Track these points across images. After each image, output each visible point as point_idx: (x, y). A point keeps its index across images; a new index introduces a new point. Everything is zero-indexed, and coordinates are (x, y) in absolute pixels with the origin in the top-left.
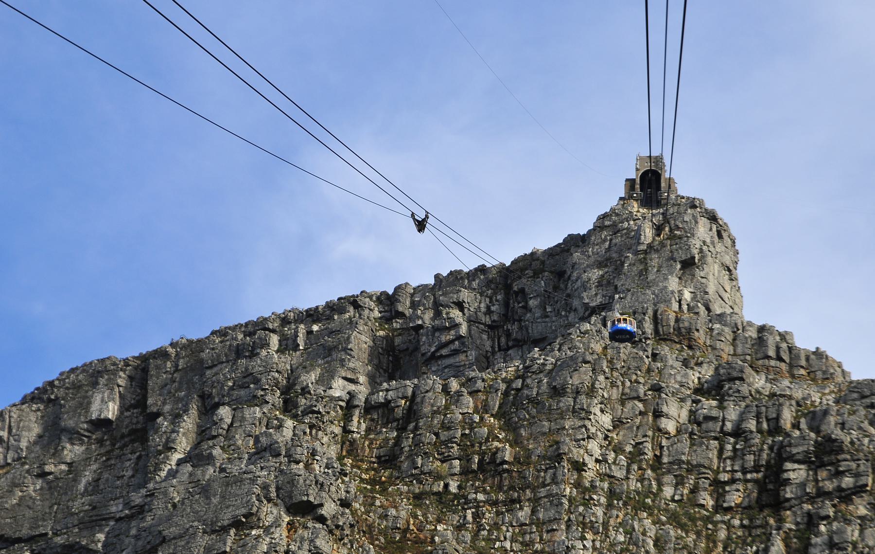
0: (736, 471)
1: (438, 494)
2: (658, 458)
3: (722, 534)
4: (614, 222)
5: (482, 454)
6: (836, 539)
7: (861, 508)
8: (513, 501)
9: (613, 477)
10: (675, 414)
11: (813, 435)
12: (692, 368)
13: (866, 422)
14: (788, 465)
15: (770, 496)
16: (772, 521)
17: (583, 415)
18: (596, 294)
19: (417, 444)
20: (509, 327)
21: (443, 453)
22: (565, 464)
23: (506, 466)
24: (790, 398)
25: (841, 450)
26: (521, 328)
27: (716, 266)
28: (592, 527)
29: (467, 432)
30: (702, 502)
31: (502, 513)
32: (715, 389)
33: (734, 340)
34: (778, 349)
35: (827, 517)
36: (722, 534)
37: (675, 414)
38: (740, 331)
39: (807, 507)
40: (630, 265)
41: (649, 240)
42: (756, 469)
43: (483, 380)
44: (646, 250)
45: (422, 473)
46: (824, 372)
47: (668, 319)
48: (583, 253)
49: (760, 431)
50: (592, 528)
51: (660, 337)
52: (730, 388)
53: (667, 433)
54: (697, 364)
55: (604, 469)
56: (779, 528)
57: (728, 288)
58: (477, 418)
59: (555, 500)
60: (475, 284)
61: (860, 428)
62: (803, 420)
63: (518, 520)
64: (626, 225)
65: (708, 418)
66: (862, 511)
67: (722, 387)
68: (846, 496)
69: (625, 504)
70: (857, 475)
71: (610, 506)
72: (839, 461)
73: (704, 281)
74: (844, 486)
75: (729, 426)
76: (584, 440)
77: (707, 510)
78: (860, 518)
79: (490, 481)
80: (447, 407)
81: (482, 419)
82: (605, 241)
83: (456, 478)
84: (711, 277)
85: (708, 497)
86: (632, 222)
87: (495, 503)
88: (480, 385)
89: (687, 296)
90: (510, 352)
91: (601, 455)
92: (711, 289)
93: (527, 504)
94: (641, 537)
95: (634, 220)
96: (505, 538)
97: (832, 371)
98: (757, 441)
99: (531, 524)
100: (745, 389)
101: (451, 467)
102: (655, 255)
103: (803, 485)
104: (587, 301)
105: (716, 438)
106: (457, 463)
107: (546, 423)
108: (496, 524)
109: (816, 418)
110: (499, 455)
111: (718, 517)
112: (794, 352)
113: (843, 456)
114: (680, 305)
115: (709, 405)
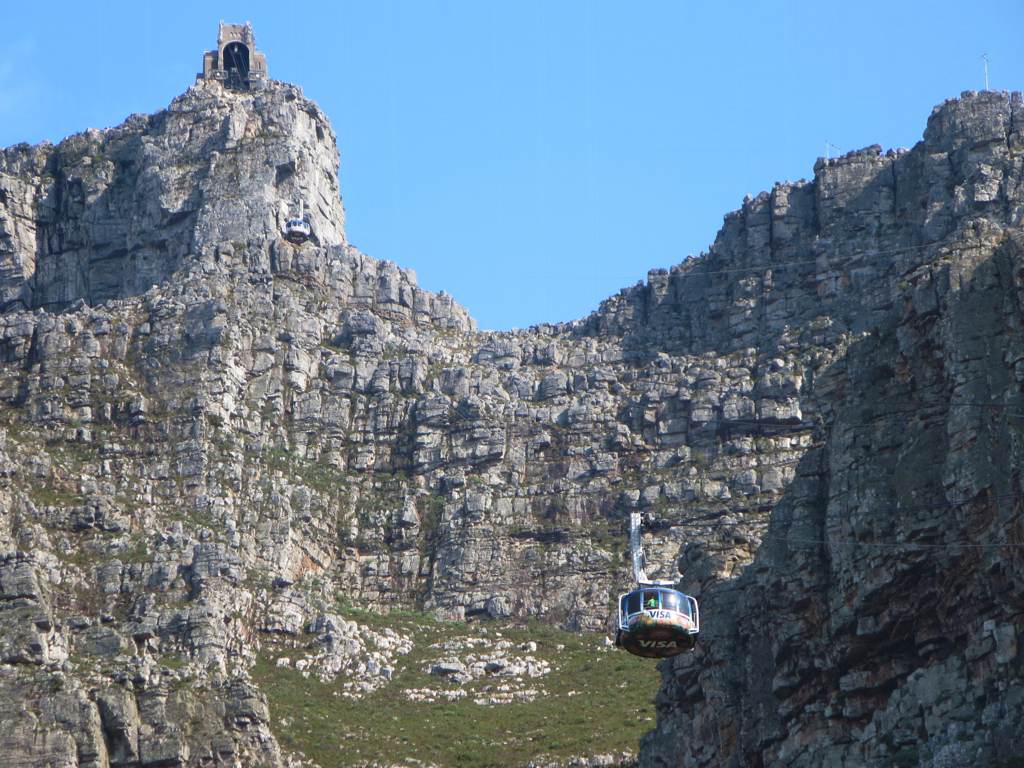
0: (369, 432)
1: (72, 441)
2: (289, 414)
3: (355, 497)
4: (195, 107)
5: (115, 403)
6: (469, 507)
7: (494, 476)
8: (150, 454)
9: (249, 433)
10: (306, 366)
11: (448, 398)
12: (317, 315)
13: (501, 386)
14: (422, 429)
15: (404, 459)
16: (404, 485)
17: (219, 367)
18: (177, 199)
19: (45, 387)
20: (63, 226)
21: (73, 399)
22: (202, 418)
23: (141, 417)
24: (421, 354)
25: (476, 416)
26: (77, 228)
27: (318, 174)
28: (231, 483)
29: (97, 377)
30: (334, 462)
31: (139, 465)
32: (347, 340)
33: (354, 279)
34: (401, 291)
35: (460, 484)
36: (355, 497)
37: (306, 366)
38: (359, 269)
39: (441, 473)
40: (217, 166)
41: (239, 136)
42: (389, 430)
43: (109, 322)
44: (235, 148)
45: (53, 419)
46: (450, 320)
47: (286, 254)
48: (156, 143)
49: (392, 390)
50: (232, 485)
51: (281, 276)
52: (362, 342)
53: (298, 387)
54: (319, 309)
55: (237, 423)
56: (412, 493)
57: (329, 201)
58: (106, 363)
59: (194, 456)
60: (17, 167)
61: (495, 393)
62: (436, 381)
63: (156, 473)
64: (208, 112)
65: (340, 375)
66: (496, 480)
67: (351, 340)
68: (480, 465)
69: (262, 461)
70: (491, 444)
71: (247, 463)
72: (474, 428)
73: (303, 191)
74: (478, 453)
75: (361, 383)
76: (220, 393)
77: (339, 471)
78: (493, 486)
79: (124, 429)
80: (73, 350)
81: (111, 364)
82: (183, 131)
83: (87, 426)
84: (311, 188)
85: (340, 458)
86: (216, 110)
87: (132, 455)
88: (105, 326)
89: (285, 209)
90: (64, 256)
91: (236, 409)
92: (312, 201)
93: (165, 457)
94: (280, 496)
95: (219, 108)
96: (145, 490)
97: (457, 319)
98: (390, 401)
99: (171, 477)
100: (377, 345)
101: (82, 414)
102: (247, 157)
103: (437, 451)
104: (166, 206)
105: (347, 396)
106: (88, 410)
107: (182, 375)
108: (135, 476)
109: (452, 380)
110: (133, 405)
111: (350, 479)
112: (418, 295)
113: (479, 423)
114: (277, 221)
115: (339, 360)
